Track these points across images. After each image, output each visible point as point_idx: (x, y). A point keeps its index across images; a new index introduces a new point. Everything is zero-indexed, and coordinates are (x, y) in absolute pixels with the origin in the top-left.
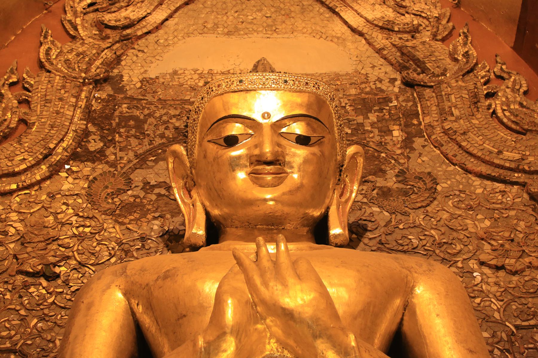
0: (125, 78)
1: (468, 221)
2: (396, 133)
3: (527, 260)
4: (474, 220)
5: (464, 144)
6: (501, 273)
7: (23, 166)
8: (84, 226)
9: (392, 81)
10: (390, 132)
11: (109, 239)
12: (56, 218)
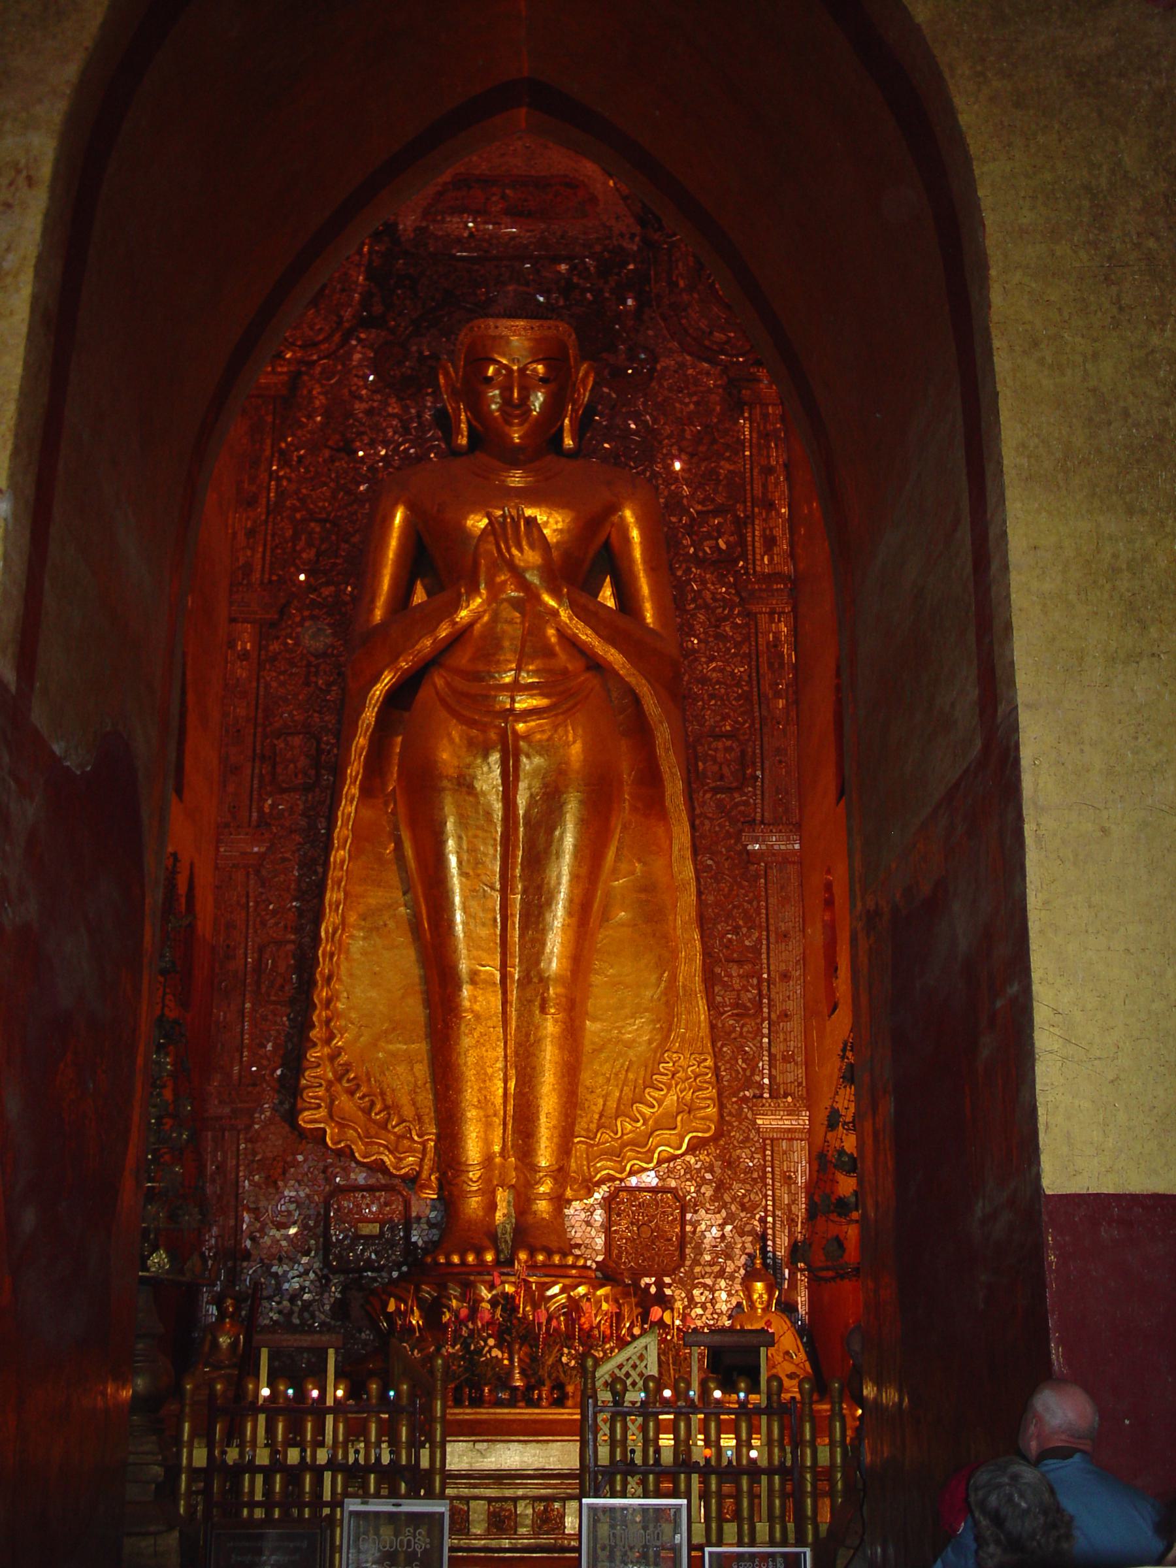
0: (401, 227)
1: (677, 405)
2: (630, 302)
3: (715, 447)
4: (682, 403)
5: (684, 321)
6: (695, 460)
7: (321, 337)
8: (374, 401)
9: (633, 236)
10: (624, 303)
11: (393, 416)
12: (350, 391)
